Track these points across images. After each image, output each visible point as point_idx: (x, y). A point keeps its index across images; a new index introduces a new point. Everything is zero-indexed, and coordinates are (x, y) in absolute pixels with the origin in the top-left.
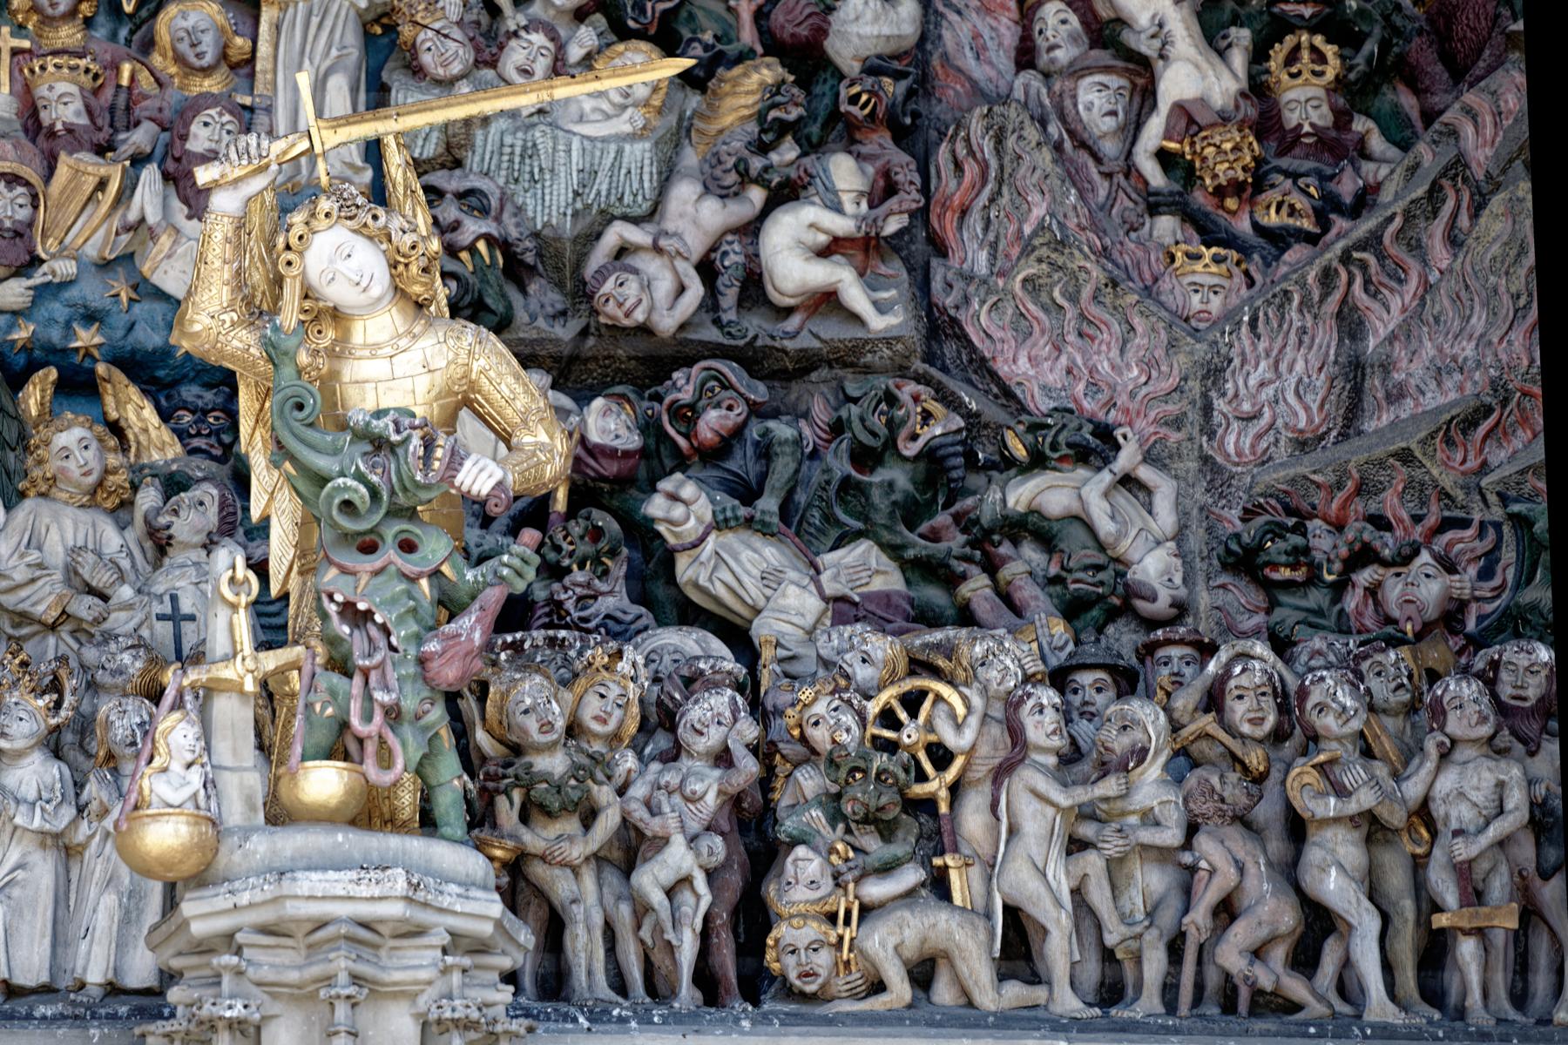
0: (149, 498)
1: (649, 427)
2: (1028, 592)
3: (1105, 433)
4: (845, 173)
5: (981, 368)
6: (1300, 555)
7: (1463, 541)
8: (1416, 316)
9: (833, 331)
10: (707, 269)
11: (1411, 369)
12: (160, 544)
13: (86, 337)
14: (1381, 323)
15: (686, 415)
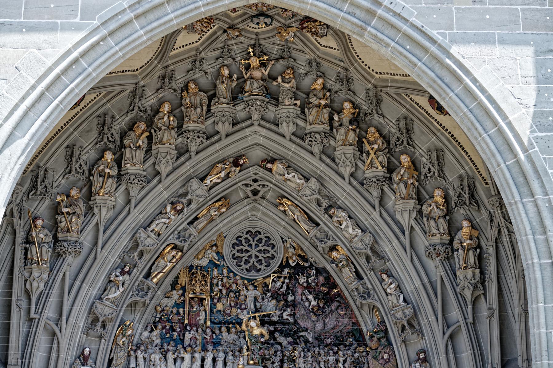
0: (239, 334)
1: (274, 328)
2: (302, 341)
3: (307, 329)
4: (289, 310)
5: (298, 324)
6: (321, 339)
7: (332, 337)
8: (329, 321)
9: (288, 321)
10: (279, 316)
11: (328, 325)
12: (239, 337)
13: (234, 321)
14: (326, 321)
15: (277, 328)
